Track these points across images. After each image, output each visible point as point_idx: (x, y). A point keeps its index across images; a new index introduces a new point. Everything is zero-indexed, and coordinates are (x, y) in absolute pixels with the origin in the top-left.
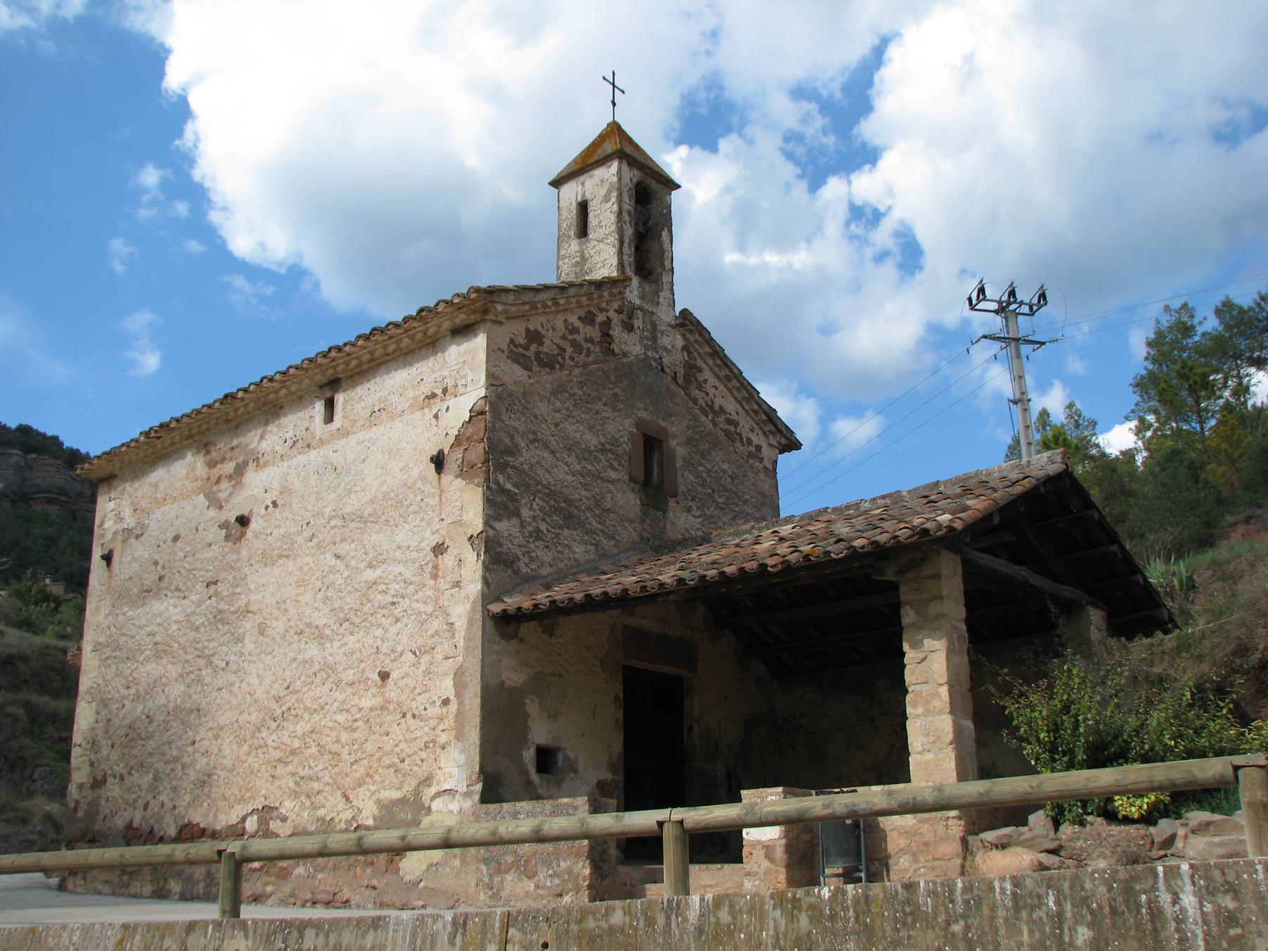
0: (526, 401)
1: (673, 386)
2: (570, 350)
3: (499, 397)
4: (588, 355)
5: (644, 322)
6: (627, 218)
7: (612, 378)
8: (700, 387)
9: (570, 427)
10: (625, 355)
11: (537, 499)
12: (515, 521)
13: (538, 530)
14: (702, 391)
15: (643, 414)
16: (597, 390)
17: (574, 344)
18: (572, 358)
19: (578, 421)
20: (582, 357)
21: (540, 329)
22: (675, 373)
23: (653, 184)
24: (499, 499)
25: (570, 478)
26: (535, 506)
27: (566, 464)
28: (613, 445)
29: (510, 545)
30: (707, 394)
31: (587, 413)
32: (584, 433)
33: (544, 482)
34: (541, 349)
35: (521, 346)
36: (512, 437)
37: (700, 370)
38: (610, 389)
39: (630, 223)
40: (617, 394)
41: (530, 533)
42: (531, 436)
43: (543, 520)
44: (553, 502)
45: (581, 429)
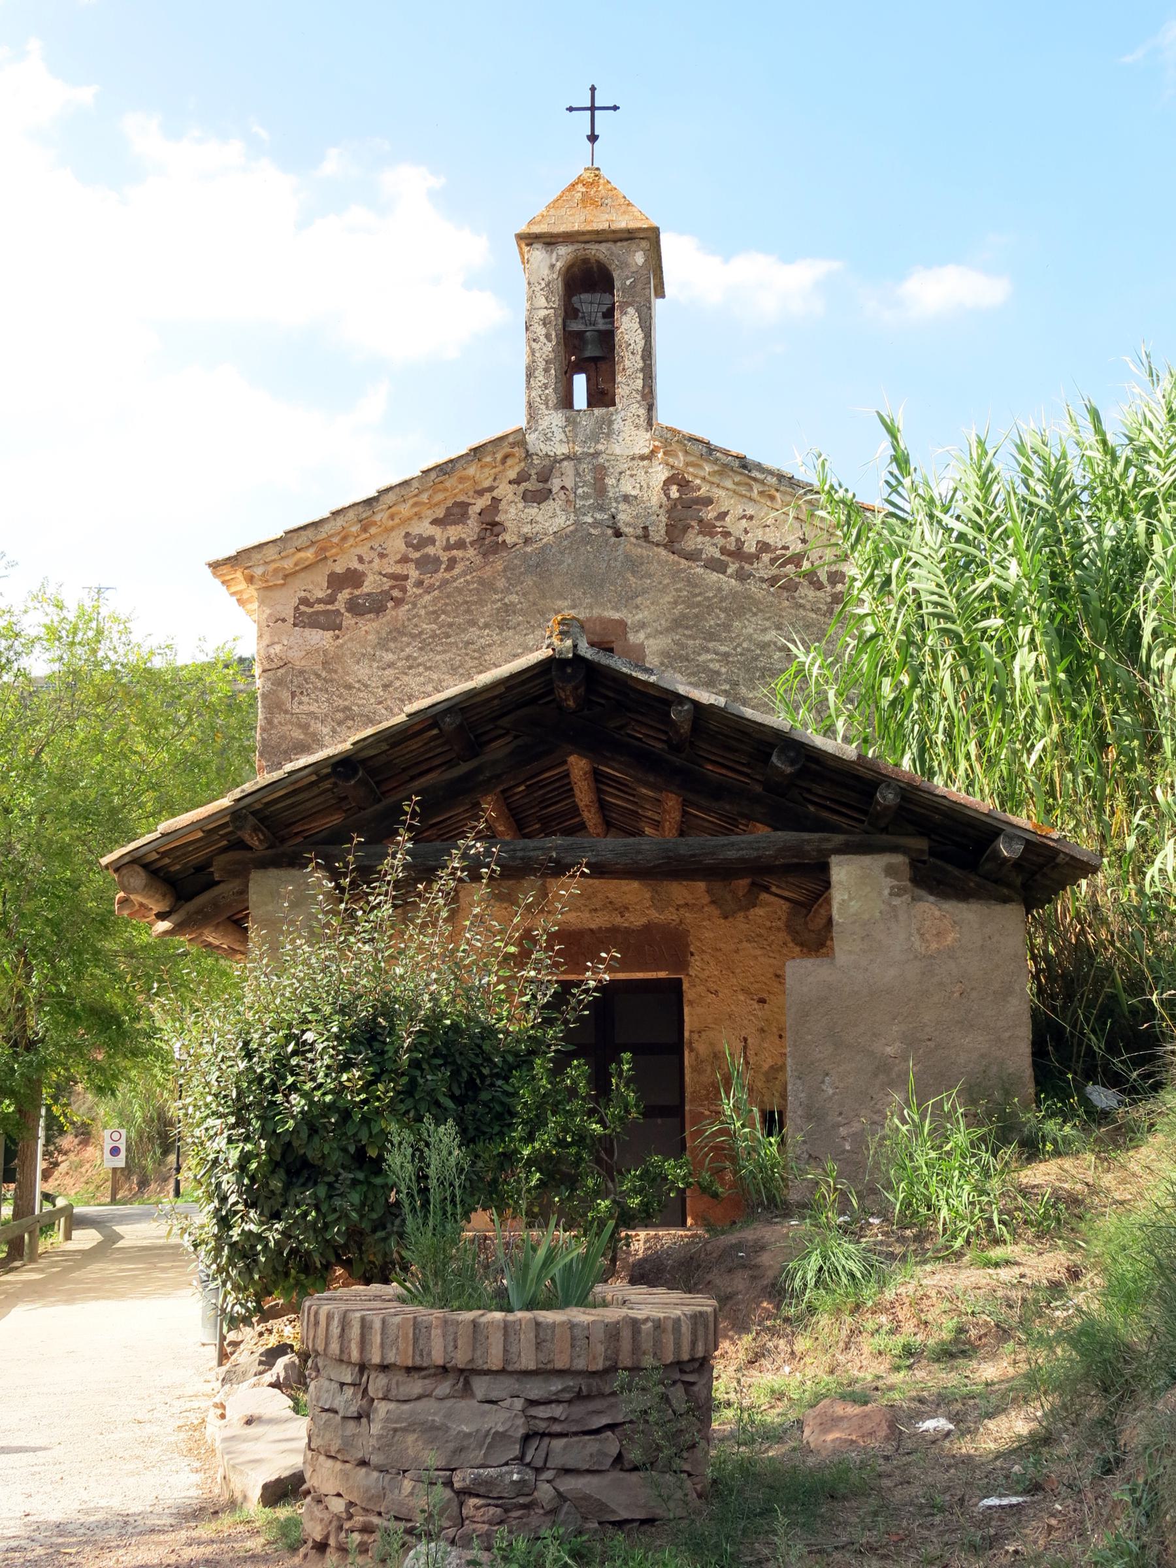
0: (330, 671)
1: (642, 551)
2: (414, 574)
3: (279, 682)
4: (449, 568)
5: (578, 474)
6: (540, 331)
7: (501, 583)
8: (707, 529)
10: (527, 541)
14: (712, 535)
16: (468, 611)
17: (420, 563)
18: (419, 584)
19: (428, 669)
20: (439, 575)
21: (355, 565)
22: (645, 528)
23: (600, 252)
30: (727, 534)
31: (444, 652)
34: (357, 592)
35: (319, 601)
36: (305, 727)
37: (708, 501)
38: (494, 602)
39: (548, 336)
40: (512, 603)
42: (339, 716)
45: (435, 677)
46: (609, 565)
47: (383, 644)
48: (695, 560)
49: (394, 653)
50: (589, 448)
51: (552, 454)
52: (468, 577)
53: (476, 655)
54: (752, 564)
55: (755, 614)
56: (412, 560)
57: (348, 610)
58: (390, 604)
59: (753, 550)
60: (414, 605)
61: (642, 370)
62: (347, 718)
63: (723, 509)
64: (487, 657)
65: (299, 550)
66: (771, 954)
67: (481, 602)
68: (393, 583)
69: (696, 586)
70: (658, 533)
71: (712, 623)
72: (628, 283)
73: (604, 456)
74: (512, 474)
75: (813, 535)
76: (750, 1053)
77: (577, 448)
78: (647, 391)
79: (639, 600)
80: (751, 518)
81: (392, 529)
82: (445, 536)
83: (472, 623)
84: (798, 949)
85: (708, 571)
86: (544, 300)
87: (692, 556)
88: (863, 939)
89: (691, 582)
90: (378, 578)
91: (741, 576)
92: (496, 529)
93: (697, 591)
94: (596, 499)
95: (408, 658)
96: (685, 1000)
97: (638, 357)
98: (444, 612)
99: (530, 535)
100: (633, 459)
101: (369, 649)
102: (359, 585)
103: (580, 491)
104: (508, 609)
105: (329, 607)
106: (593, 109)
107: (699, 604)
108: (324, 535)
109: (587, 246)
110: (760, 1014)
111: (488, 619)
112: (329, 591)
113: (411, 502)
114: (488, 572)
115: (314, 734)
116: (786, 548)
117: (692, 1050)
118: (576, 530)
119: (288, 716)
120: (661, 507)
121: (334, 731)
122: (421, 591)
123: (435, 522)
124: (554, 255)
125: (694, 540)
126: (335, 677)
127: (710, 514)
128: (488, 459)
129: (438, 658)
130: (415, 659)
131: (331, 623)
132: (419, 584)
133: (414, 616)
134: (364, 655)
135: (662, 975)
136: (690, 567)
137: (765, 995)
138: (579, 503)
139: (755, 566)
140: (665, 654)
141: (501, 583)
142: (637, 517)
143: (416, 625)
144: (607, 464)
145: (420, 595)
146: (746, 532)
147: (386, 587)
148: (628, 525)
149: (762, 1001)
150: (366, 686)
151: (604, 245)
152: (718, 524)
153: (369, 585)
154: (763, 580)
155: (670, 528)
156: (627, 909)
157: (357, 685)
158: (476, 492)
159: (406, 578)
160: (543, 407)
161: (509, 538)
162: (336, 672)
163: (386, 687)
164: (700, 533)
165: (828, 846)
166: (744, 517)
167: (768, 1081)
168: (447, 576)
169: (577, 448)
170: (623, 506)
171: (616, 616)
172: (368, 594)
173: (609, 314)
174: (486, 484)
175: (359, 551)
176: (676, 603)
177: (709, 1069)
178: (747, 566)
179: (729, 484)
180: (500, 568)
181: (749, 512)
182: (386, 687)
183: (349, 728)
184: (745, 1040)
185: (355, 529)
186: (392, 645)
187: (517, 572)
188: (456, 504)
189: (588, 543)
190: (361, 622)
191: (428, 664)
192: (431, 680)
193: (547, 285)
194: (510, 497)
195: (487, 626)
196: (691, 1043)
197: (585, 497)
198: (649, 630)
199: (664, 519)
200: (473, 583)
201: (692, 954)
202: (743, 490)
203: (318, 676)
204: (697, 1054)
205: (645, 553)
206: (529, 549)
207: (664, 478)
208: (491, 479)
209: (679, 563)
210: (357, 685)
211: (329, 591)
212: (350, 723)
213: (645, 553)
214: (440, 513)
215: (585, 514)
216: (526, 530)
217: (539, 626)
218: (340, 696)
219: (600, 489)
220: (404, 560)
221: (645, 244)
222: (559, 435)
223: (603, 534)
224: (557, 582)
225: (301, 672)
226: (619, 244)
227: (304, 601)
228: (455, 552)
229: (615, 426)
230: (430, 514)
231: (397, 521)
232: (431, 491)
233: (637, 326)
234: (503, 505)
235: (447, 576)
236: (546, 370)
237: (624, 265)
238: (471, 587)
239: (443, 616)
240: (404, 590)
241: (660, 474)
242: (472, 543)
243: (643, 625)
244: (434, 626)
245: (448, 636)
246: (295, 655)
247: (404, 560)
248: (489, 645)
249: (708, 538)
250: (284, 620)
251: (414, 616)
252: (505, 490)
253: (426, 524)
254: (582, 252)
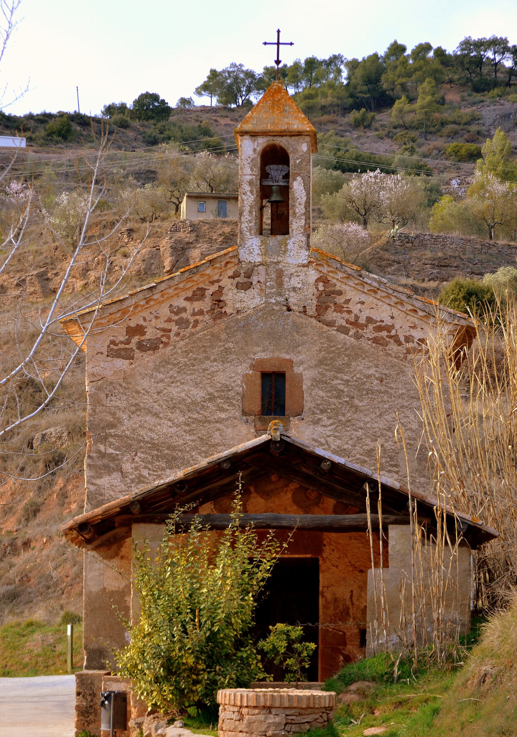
0: (128, 383)
1: (303, 320)
2: (175, 328)
3: (99, 389)
4: (195, 326)
5: (267, 274)
7: (223, 336)
8: (339, 309)
9: (175, 391)
10: (238, 312)
11: (138, 454)
12: (116, 475)
13: (141, 476)
14: (341, 312)
15: (261, 355)
16: (205, 352)
19: (183, 383)
20: (189, 330)
21: (141, 322)
23: (283, 142)
24: (100, 463)
25: (174, 430)
26: (137, 459)
27: (169, 420)
28: (222, 391)
29: (112, 493)
30: (349, 312)
31: (192, 374)
32: (189, 391)
33: (147, 439)
34: (143, 338)
35: (122, 342)
36: (114, 414)
37: (340, 293)
38: (219, 347)
39: (251, 192)
40: (229, 348)
41: (132, 481)
42: (133, 408)
43: (145, 467)
44: (156, 452)
45: (186, 388)
46: (284, 328)
47: (157, 369)
48: (332, 326)
49: (163, 374)
50: (274, 259)
51: (253, 261)
52: (205, 332)
53: (209, 376)
54: (363, 330)
55: (364, 359)
56: (173, 321)
57: (138, 348)
58: (161, 346)
59: (364, 322)
60: (175, 347)
61: (305, 214)
62: (137, 410)
63: (348, 298)
64: (215, 378)
65: (111, 314)
67: (212, 347)
68: (162, 333)
69: (332, 341)
70: (312, 311)
71: (340, 362)
72: (298, 162)
73: (282, 264)
74: (230, 273)
75: (397, 314)
76: (354, 599)
77: (267, 259)
78: (307, 226)
79: (300, 348)
80: (363, 303)
81: (162, 302)
82: (192, 307)
83: (207, 358)
85: (339, 333)
86: (249, 170)
87: (330, 324)
88: (401, 561)
89: (329, 339)
90: (154, 330)
91: (357, 336)
92: (221, 304)
93: (332, 344)
94: (277, 289)
95: (171, 377)
96: (320, 570)
97: (303, 207)
98: (191, 352)
99: (240, 309)
100: (298, 266)
101: (149, 371)
102: (144, 333)
103: (268, 284)
104: (227, 351)
105: (127, 346)
106: (278, 44)
107: (333, 352)
108: (125, 306)
109: (275, 138)
110: (360, 579)
111: (216, 357)
112: (127, 337)
113: (173, 288)
114: (216, 330)
115: (119, 419)
116: (382, 321)
117: (323, 596)
118: (266, 307)
119: (104, 408)
120: (313, 295)
121: (130, 417)
122: (179, 339)
123: (187, 299)
124: (256, 144)
125: (331, 315)
126: (130, 386)
127: (340, 300)
128: (218, 265)
129: (188, 377)
130: (175, 378)
131: (128, 355)
132: (178, 334)
133: (175, 353)
134: (146, 374)
135: (308, 556)
136: (328, 330)
137: (363, 568)
138: (268, 291)
139: (365, 331)
140: (314, 380)
141: (223, 336)
142: (300, 300)
143: (176, 359)
144: (283, 269)
145: (178, 341)
146: (361, 311)
147: (159, 336)
148: (295, 305)
150: (148, 392)
151: (284, 138)
152: (345, 306)
153: (150, 334)
154: (369, 339)
155: (318, 308)
157: (142, 392)
158: (209, 282)
159: (170, 331)
160: (249, 233)
161: (228, 310)
162: (131, 383)
163: (159, 393)
164: (335, 310)
165: (388, 521)
166: (360, 302)
168: (193, 330)
169: (267, 259)
170: (292, 294)
171: (288, 357)
172: (149, 340)
173: (287, 176)
174: (216, 278)
175: (144, 314)
176: (320, 351)
177: (332, 607)
178: (360, 331)
179: (351, 284)
180: (223, 327)
181: (363, 299)
182: (159, 393)
183: (138, 416)
184: (352, 592)
185: (142, 303)
186: (162, 369)
187: (233, 329)
188: (199, 289)
189: (272, 315)
190: (145, 355)
191: (183, 381)
192: (184, 390)
193: (252, 161)
194: (229, 286)
195: (215, 360)
196: (323, 593)
197: (271, 287)
198: (305, 365)
199: (315, 302)
200: (208, 335)
201: (325, 546)
202: (359, 287)
203: (121, 385)
205: (304, 321)
206: (239, 317)
207: (315, 278)
208: (218, 275)
209: (323, 328)
210: (142, 392)
211: (127, 337)
212: (139, 413)
213: (304, 321)
214: (190, 294)
215: (271, 298)
216: (237, 306)
217: (244, 361)
218: (133, 397)
219: (280, 284)
220: (169, 320)
221: (308, 139)
222: (257, 251)
223: (281, 310)
224: (255, 336)
225: (111, 383)
226: (293, 138)
227: (113, 342)
228: (197, 317)
229: (289, 247)
230: (184, 295)
231: (165, 297)
232: (185, 283)
233: (302, 188)
234: (225, 291)
235: (193, 330)
236: (250, 212)
237: (296, 151)
238: (207, 338)
239: (191, 354)
240: (169, 337)
241: (313, 275)
242: (208, 312)
243: (302, 363)
244: (186, 360)
245: (194, 366)
246: (108, 373)
247: (169, 320)
248: (217, 371)
249: (339, 314)
250: (102, 353)
251: (175, 353)
252: (226, 282)
253: (182, 300)
254: (271, 143)
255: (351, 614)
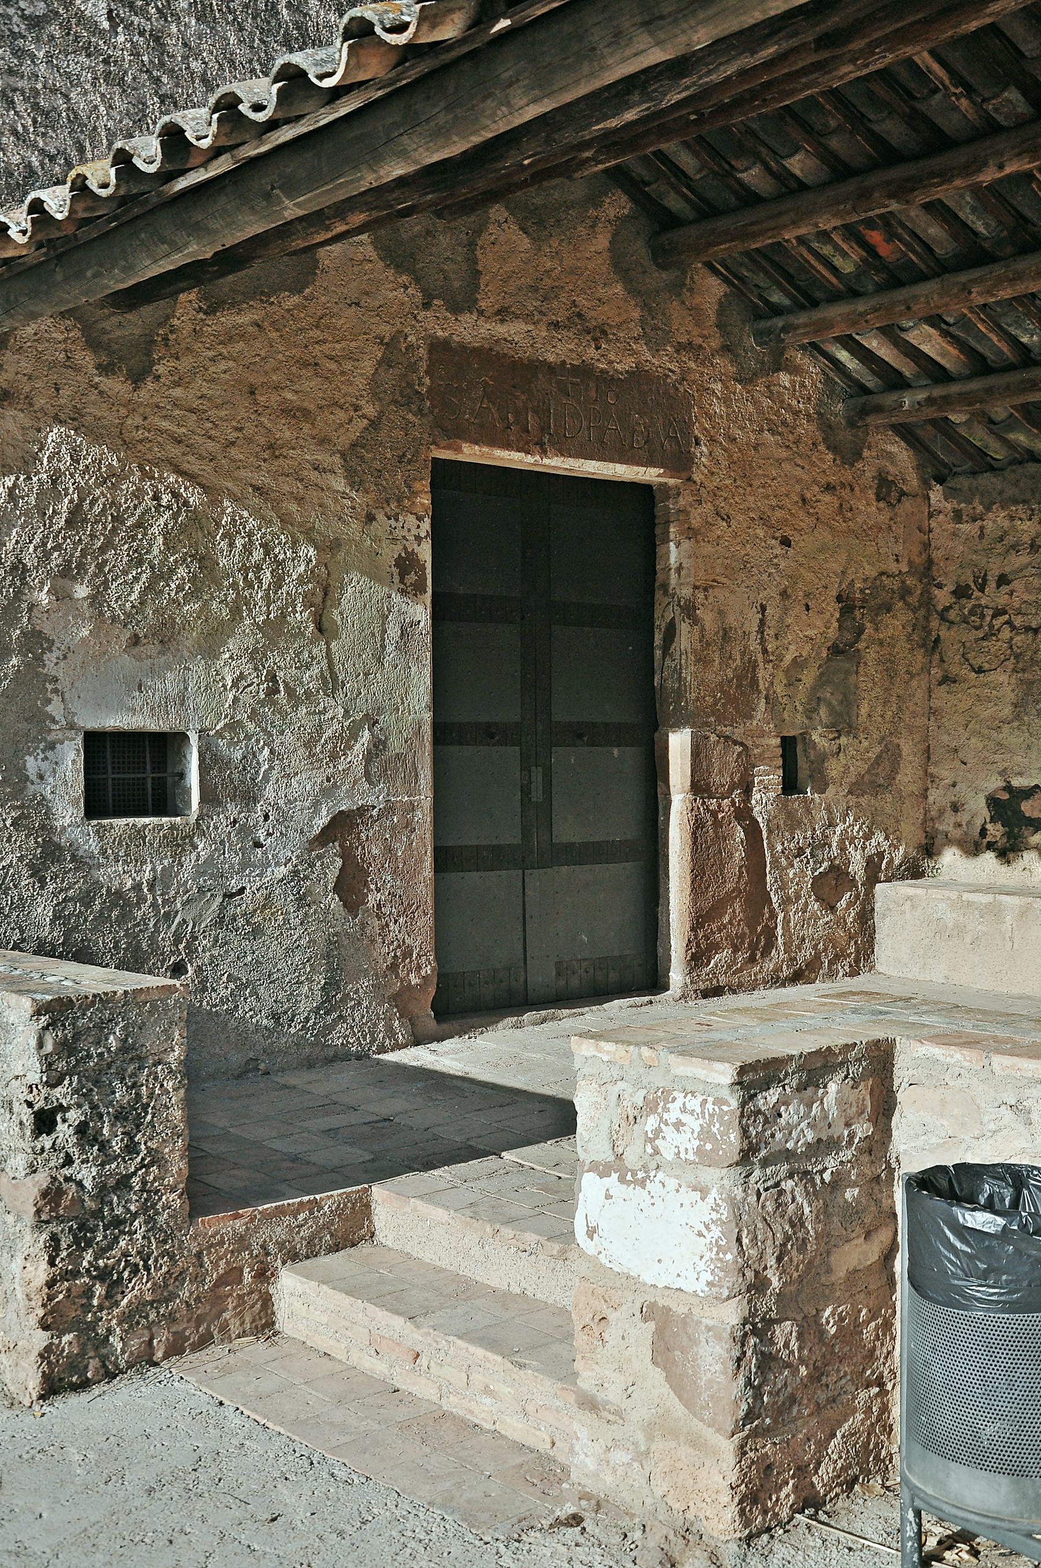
66: (799, 461)
76: (770, 632)
84: (830, 456)
137: (788, 532)
149: (786, 542)
156: (604, 333)
167: (789, 685)
184: (763, 608)
204: (703, 629)
255: (761, 687)
